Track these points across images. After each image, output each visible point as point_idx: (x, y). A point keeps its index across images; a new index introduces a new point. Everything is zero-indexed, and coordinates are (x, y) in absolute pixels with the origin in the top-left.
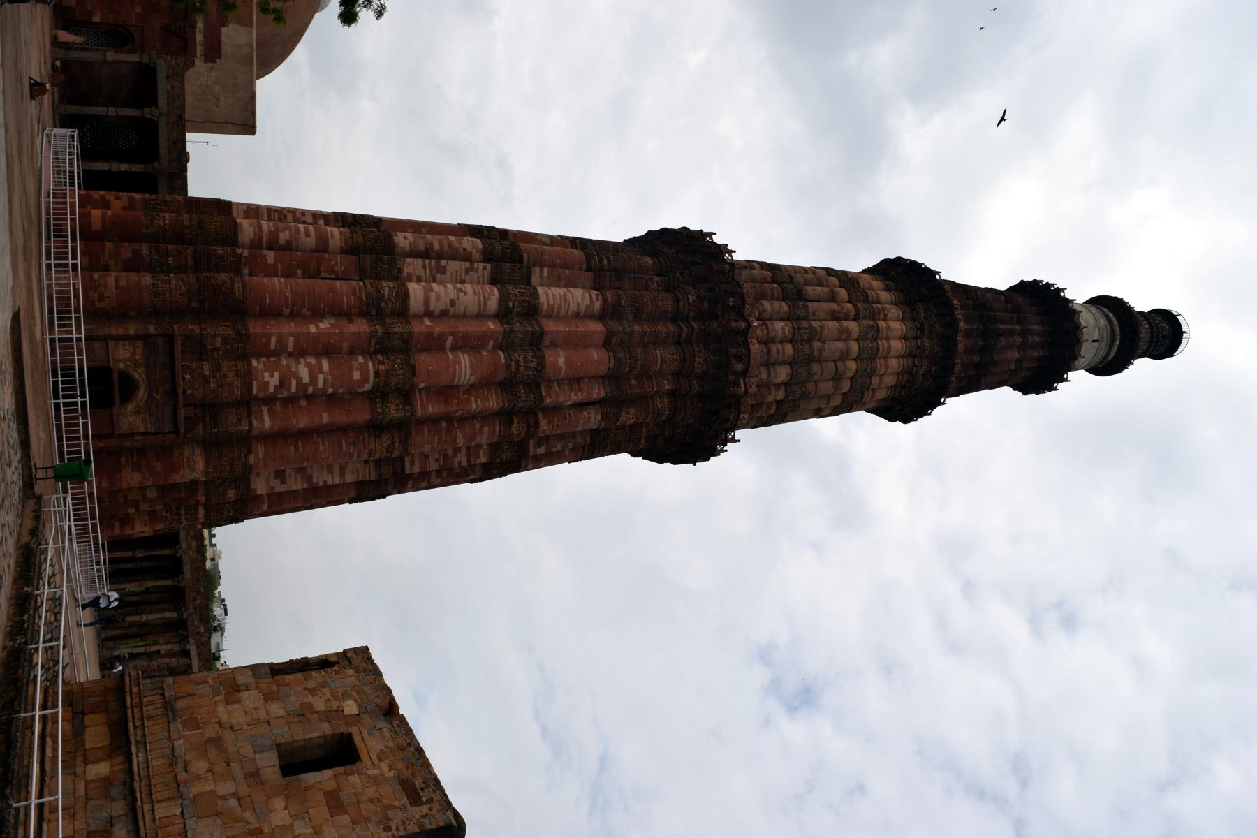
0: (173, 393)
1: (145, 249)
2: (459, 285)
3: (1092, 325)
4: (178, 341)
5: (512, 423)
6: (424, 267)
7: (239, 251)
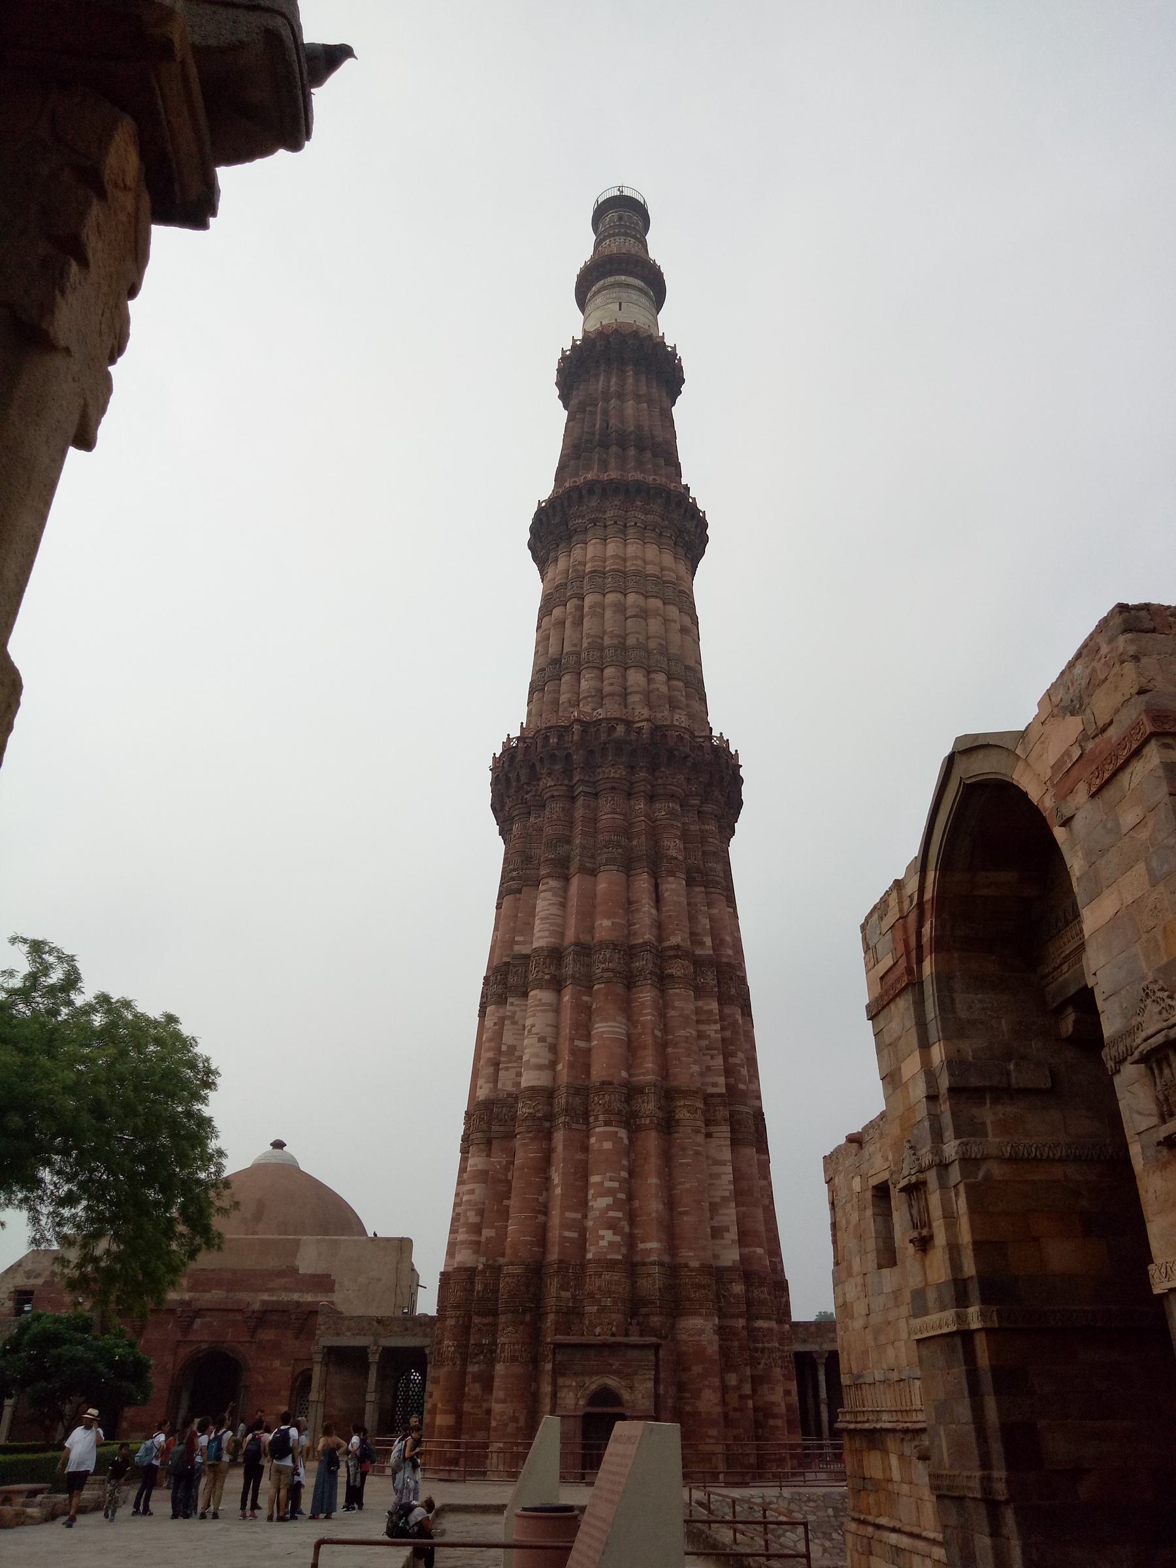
0: (613, 1348)
1: (473, 1369)
4: (560, 1338)
5: (671, 975)
6: (507, 1069)
7: (480, 1267)
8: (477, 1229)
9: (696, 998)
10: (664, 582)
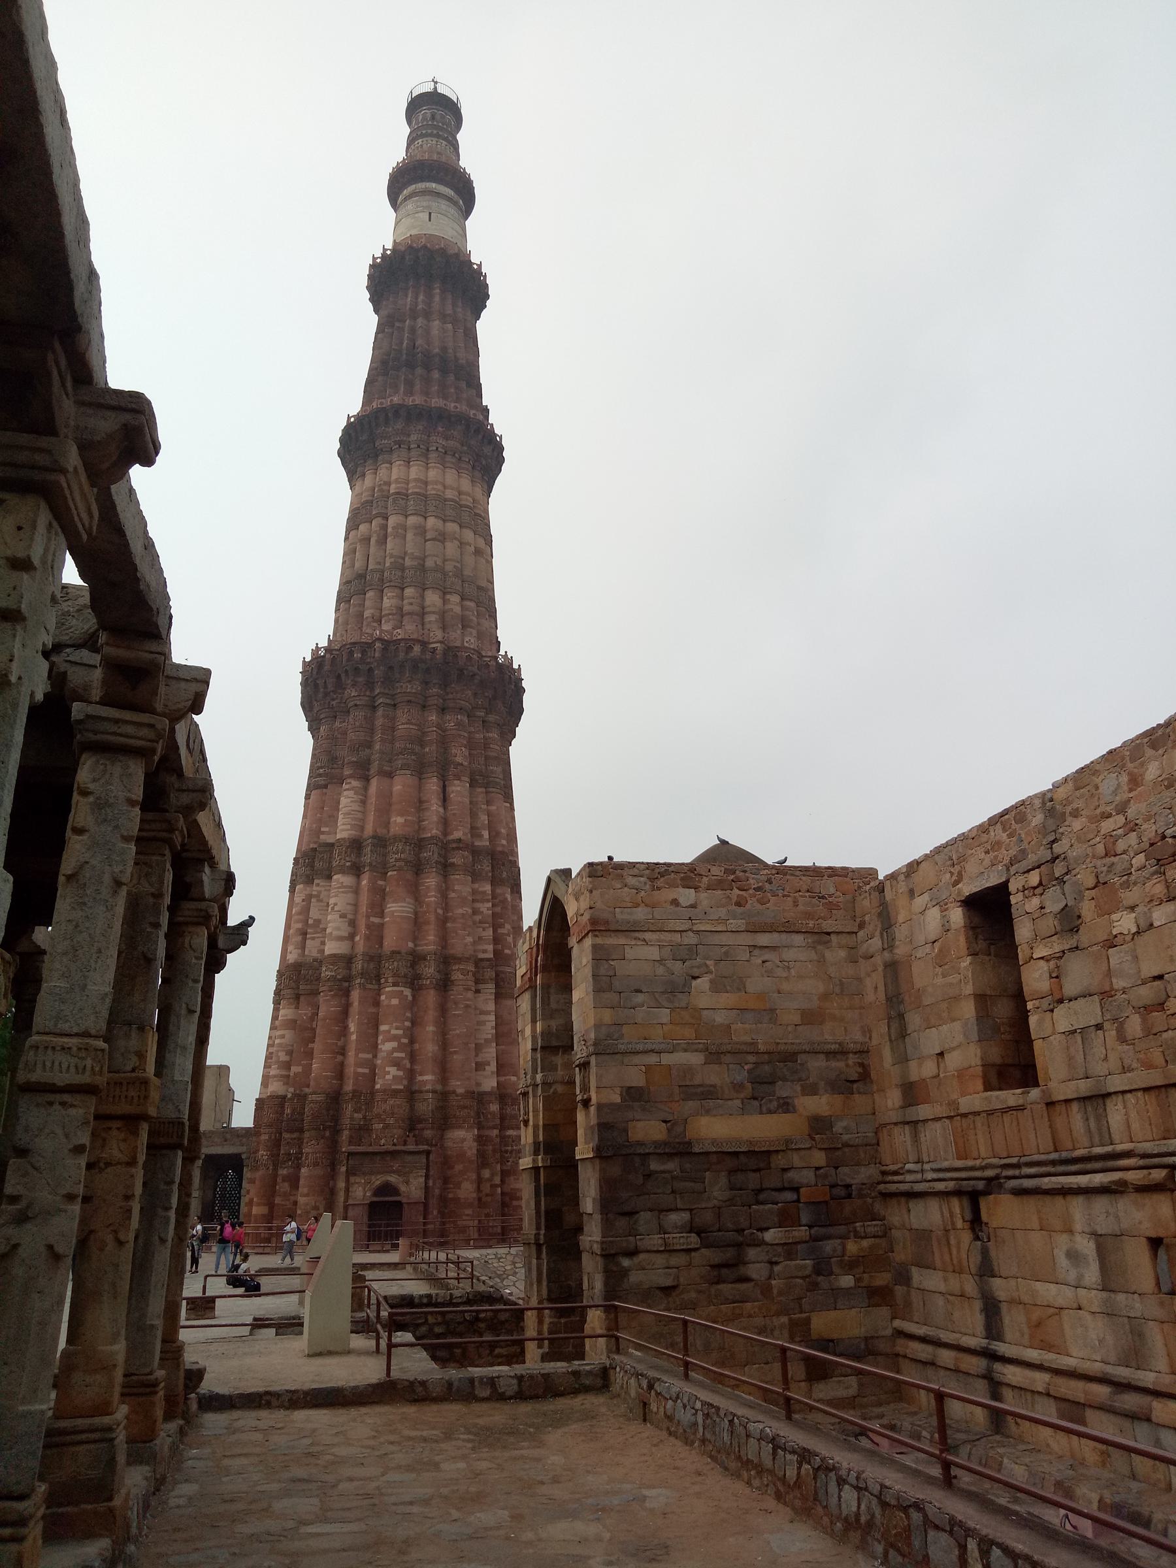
0: (393, 1154)
1: (283, 1172)
4: (353, 1148)
5: (453, 864)
6: (313, 939)
7: (289, 1096)
8: (287, 1066)
10: (461, 506)
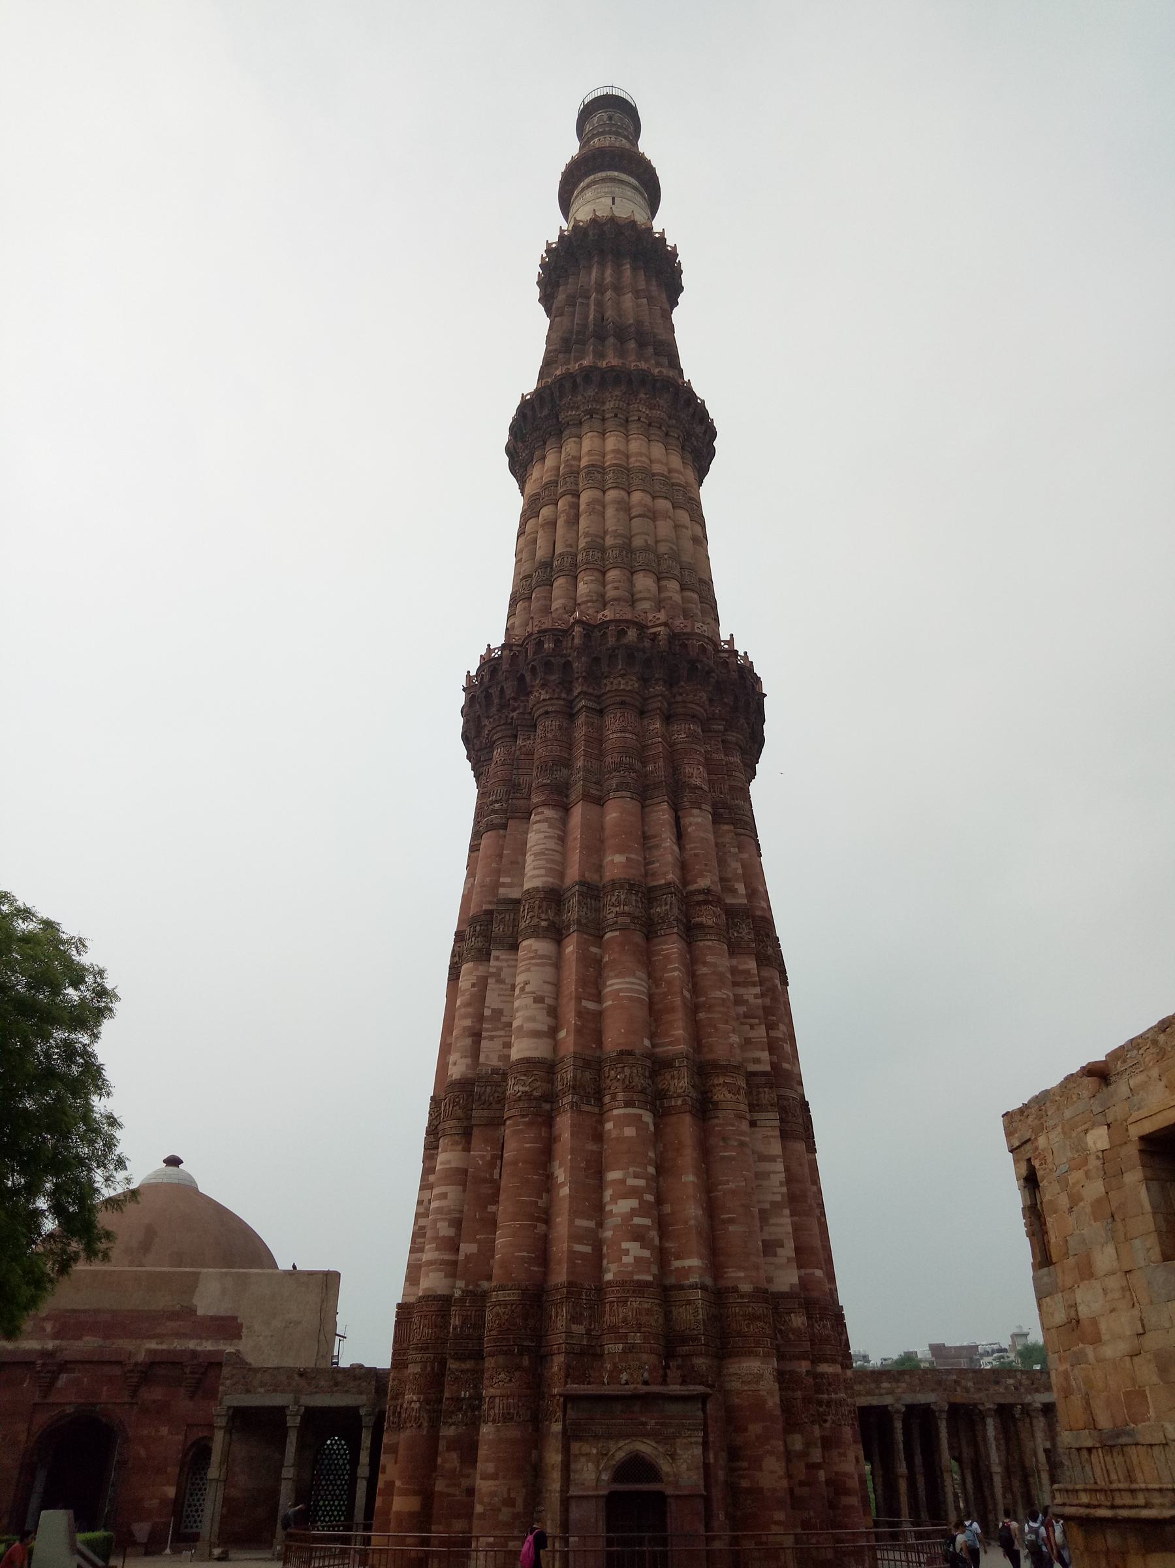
1: (448, 1432)
2: (517, 991)
3: (593, 204)
4: (575, 1388)
5: (700, 926)
6: (492, 1038)
7: (458, 1294)
8: (452, 1245)
9: (732, 954)
10: (673, 485)
